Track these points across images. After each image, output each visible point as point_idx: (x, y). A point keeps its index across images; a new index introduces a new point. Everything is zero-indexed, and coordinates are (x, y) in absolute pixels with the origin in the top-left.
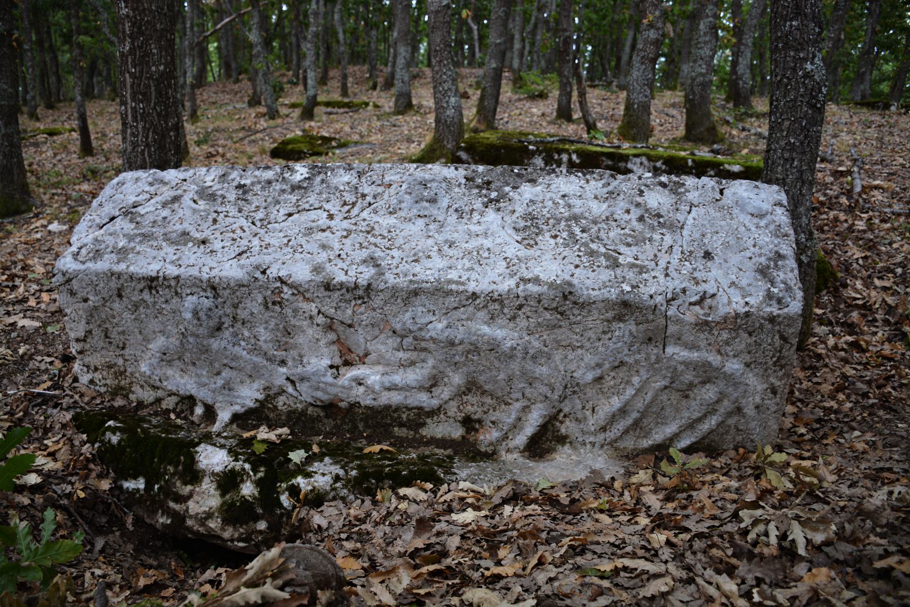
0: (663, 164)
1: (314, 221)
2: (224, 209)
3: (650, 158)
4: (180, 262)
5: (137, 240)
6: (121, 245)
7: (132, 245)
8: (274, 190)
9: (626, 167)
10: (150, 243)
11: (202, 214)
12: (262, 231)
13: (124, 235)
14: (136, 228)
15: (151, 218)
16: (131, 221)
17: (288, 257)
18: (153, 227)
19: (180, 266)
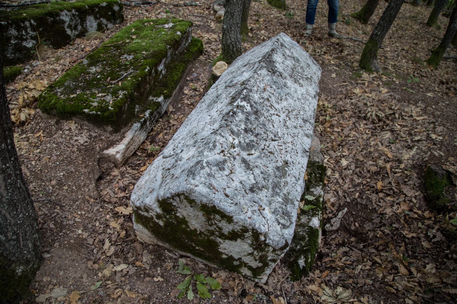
0: (75, 11)
1: (280, 122)
2: (263, 145)
3: (69, 11)
4: (297, 177)
5: (279, 191)
6: (280, 200)
7: (281, 194)
8: (254, 121)
9: (60, 19)
10: (282, 186)
11: (263, 155)
12: (282, 140)
13: (273, 197)
14: (268, 189)
15: (260, 179)
16: (261, 190)
17: (300, 140)
18: (268, 181)
19: (299, 178)
